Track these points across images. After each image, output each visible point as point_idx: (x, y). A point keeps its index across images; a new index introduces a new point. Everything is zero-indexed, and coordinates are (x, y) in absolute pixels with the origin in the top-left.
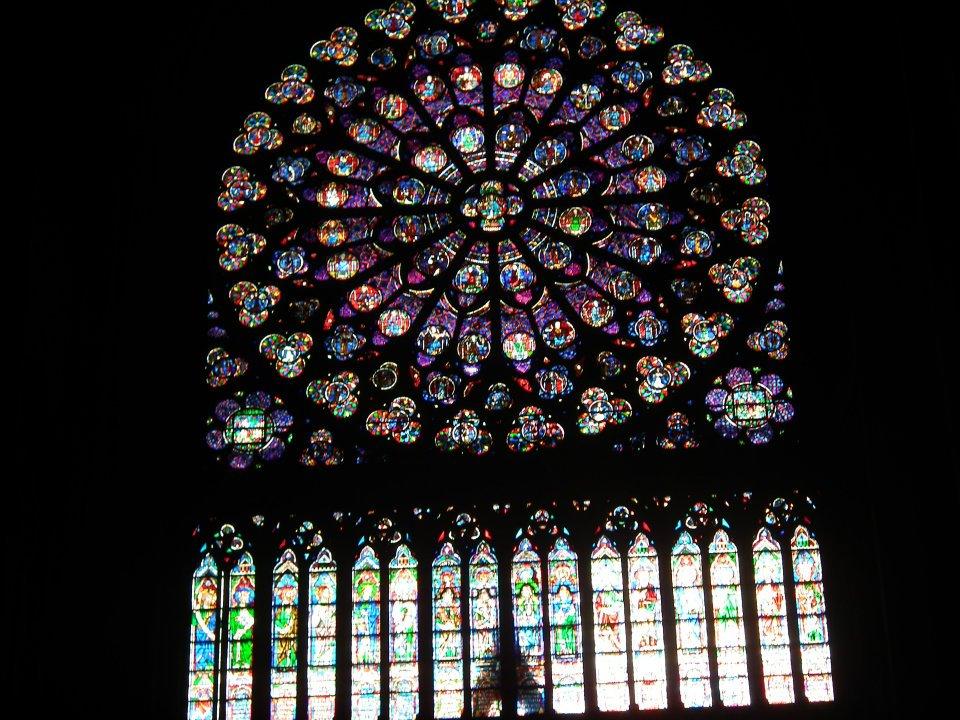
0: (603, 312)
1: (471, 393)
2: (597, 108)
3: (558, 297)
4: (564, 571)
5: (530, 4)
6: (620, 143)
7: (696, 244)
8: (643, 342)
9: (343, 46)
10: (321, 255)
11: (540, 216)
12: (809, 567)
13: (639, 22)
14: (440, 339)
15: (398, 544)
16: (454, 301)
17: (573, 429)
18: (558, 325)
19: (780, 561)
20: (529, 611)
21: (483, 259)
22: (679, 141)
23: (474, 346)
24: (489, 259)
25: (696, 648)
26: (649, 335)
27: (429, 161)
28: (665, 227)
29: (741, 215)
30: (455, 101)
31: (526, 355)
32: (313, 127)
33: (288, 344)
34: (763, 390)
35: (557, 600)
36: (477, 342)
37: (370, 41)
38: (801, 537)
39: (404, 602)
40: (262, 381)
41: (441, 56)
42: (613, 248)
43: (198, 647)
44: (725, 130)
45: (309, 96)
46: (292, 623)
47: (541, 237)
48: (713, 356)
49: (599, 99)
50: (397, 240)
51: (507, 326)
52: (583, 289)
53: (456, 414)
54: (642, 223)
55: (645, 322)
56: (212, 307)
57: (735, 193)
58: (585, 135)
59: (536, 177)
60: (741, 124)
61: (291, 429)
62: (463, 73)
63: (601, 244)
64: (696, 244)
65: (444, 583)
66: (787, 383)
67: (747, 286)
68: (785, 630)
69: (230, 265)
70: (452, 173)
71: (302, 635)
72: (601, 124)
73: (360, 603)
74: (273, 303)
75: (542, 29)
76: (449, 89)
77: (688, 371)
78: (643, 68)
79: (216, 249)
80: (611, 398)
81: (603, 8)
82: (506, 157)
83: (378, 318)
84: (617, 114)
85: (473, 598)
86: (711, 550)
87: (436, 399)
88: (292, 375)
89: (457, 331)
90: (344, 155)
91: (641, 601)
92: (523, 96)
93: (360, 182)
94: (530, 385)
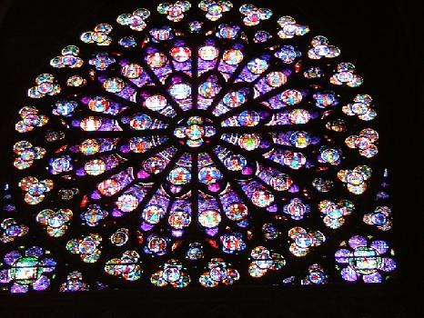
3: (237, 189)
7: (329, 157)
10: (80, 160)
16: (168, 190)
21: (188, 164)
26: (297, 214)
27: (154, 103)
31: (215, 224)
40: (36, 239)
41: (162, 42)
47: (227, 151)
49: (266, 68)
51: (201, 206)
57: (355, 125)
60: (359, 84)
61: (51, 274)
62: (178, 51)
63: (266, 156)
64: (329, 157)
66: (391, 246)
72: (268, 83)
74: (48, 190)
75: (231, 26)
79: (15, 156)
81: (271, 14)
88: (58, 235)
89: (169, 209)
92: (217, 65)
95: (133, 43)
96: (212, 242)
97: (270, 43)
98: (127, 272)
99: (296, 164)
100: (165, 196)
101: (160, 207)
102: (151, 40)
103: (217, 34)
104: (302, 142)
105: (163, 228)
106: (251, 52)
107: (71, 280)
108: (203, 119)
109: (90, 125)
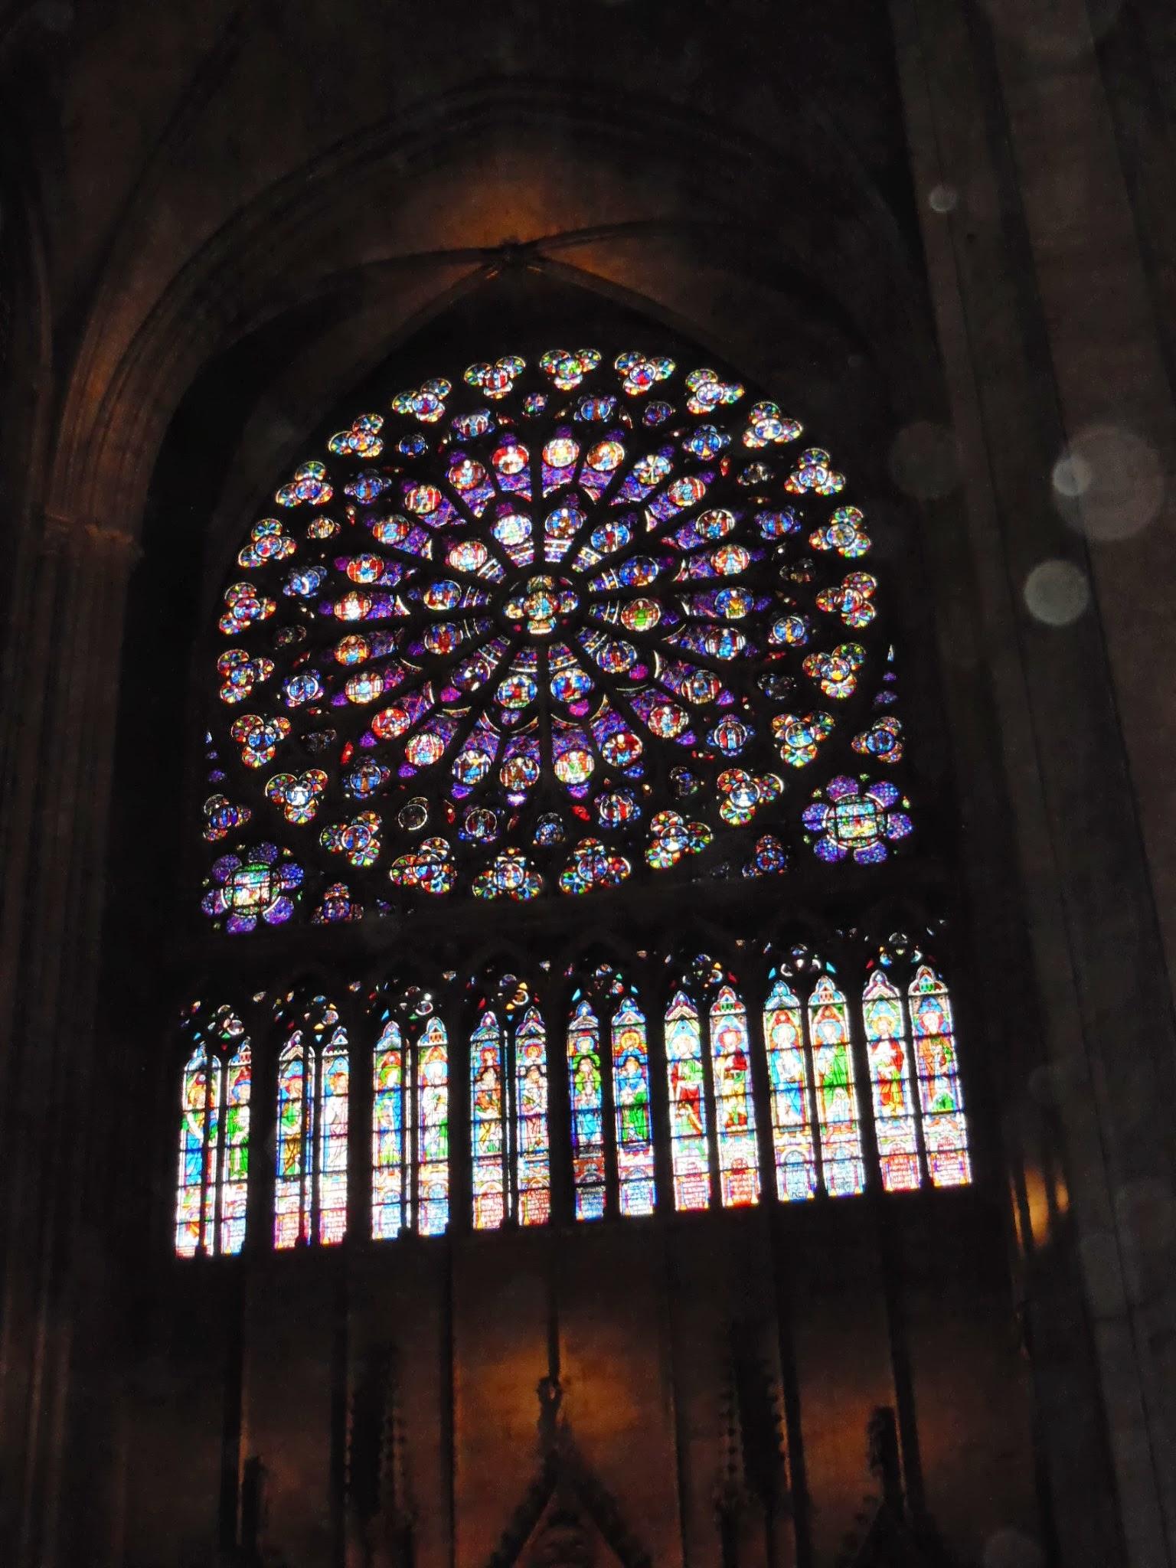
0: (676, 719)
1: (514, 828)
2: (666, 482)
3: (621, 707)
4: (630, 1040)
7: (787, 632)
10: (338, 677)
11: (599, 611)
12: (937, 1016)
14: (479, 766)
15: (429, 1017)
16: (496, 719)
18: (621, 738)
19: (900, 1011)
20: (589, 1090)
21: (530, 666)
23: (520, 770)
25: (796, 1126)
26: (732, 744)
27: (466, 558)
29: (840, 593)
30: (496, 486)
31: (582, 777)
33: (299, 783)
34: (873, 801)
35: (624, 1073)
36: (525, 767)
37: (399, 428)
38: (925, 981)
39: (435, 1086)
42: (686, 644)
43: (190, 1156)
44: (821, 496)
46: (300, 1120)
47: (600, 636)
48: (809, 766)
49: (668, 470)
50: (429, 652)
51: (559, 743)
52: (651, 694)
55: (726, 728)
56: (213, 746)
57: (835, 569)
58: (651, 515)
59: (591, 567)
60: (839, 488)
62: (506, 453)
64: (787, 632)
65: (485, 1061)
67: (850, 678)
68: (908, 1098)
71: (311, 1136)
73: (382, 1092)
74: (282, 736)
75: (601, 397)
76: (490, 474)
77: (780, 785)
78: (721, 432)
81: (671, 367)
82: (559, 546)
83: (405, 745)
84: (690, 487)
85: (520, 1077)
86: (813, 1001)
87: (474, 836)
88: (303, 820)
90: (366, 559)
91: (727, 1070)
94: (588, 813)
95: (421, 444)
96: (580, 810)
97: (672, 423)
98: (429, 876)
100: (491, 729)
101: (482, 752)
104: (736, 610)
107: (330, 900)
108: (556, 580)
109: (352, 610)
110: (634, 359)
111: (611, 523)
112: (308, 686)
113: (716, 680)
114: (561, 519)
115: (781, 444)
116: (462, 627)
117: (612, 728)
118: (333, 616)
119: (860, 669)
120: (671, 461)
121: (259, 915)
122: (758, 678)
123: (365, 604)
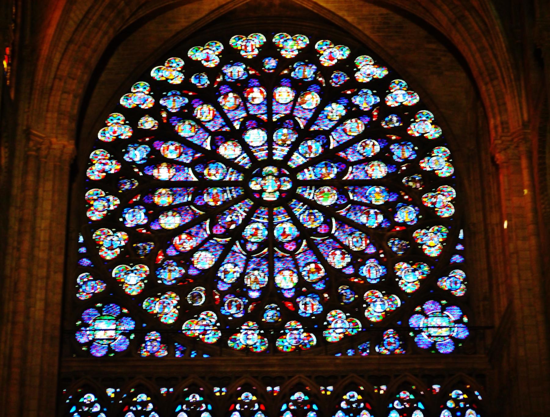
0: (343, 258)
3: (313, 248)
5: (299, 48)
6: (355, 145)
7: (406, 215)
8: (369, 280)
9: (174, 70)
10: (155, 212)
13: (372, 63)
14: (234, 272)
16: (243, 246)
17: (322, 340)
18: (313, 266)
21: (264, 218)
22: (396, 144)
23: (256, 278)
24: (268, 219)
27: (229, 150)
28: (386, 203)
30: (246, 109)
31: (291, 285)
32: (152, 125)
33: (132, 271)
34: (448, 316)
37: (192, 68)
41: (238, 81)
42: (350, 216)
44: (426, 138)
45: (149, 104)
47: (303, 206)
49: (344, 113)
50: (206, 203)
51: (278, 265)
52: (330, 242)
53: (243, 325)
54: (370, 199)
57: (432, 181)
60: (437, 136)
61: (131, 332)
62: (253, 92)
63: (343, 212)
64: (406, 215)
69: (95, 217)
70: (244, 161)
72: (344, 130)
74: (123, 243)
75: (307, 65)
77: (399, 302)
78: (374, 94)
79: (87, 205)
80: (347, 317)
83: (192, 257)
84: (356, 125)
88: (134, 293)
89: (245, 268)
90: (172, 144)
92: (293, 109)
93: (182, 163)
94: (294, 306)
95: (205, 81)
98: (204, 333)
99: (374, 220)
100: (241, 253)
101: (236, 265)
102: (224, 77)
103: (292, 75)
105: (239, 288)
106: (329, 96)
108: (279, 170)
109: (163, 173)
110: (326, 45)
111: (311, 140)
112: (138, 216)
113: (366, 238)
114: (283, 135)
115: (406, 106)
116: (225, 191)
117: (307, 259)
118: (152, 176)
119: (444, 241)
120: (346, 108)
121: (109, 344)
122: (388, 241)
123: (171, 171)
